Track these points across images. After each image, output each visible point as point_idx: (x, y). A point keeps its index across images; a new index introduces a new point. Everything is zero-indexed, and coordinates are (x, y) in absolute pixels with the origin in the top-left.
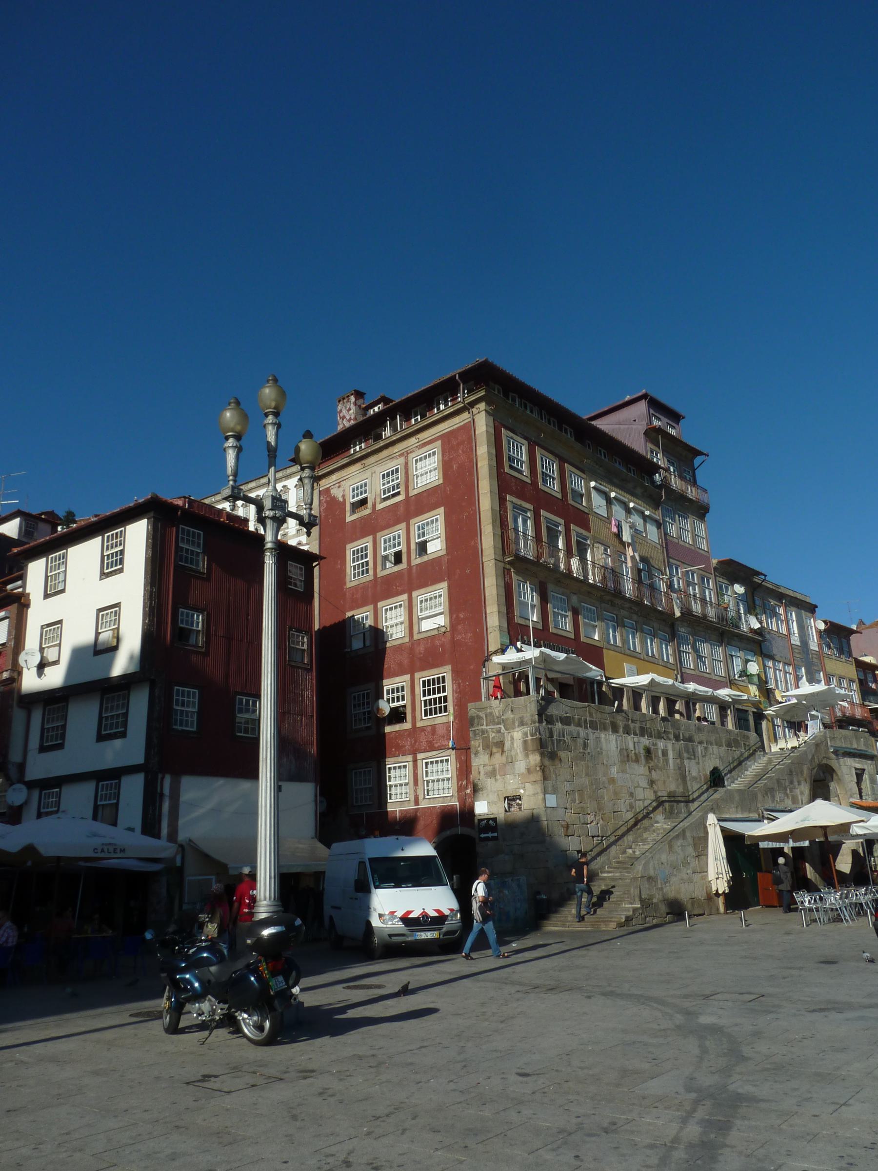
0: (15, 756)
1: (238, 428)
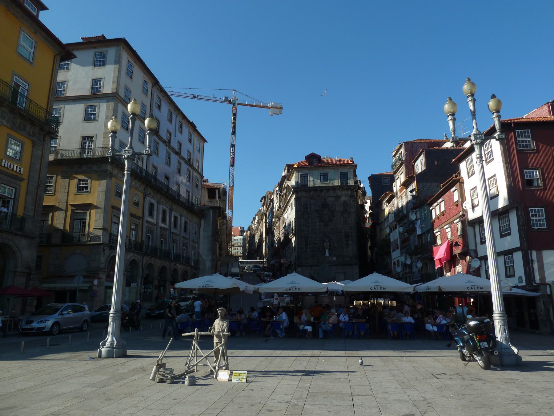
1: (452, 110)
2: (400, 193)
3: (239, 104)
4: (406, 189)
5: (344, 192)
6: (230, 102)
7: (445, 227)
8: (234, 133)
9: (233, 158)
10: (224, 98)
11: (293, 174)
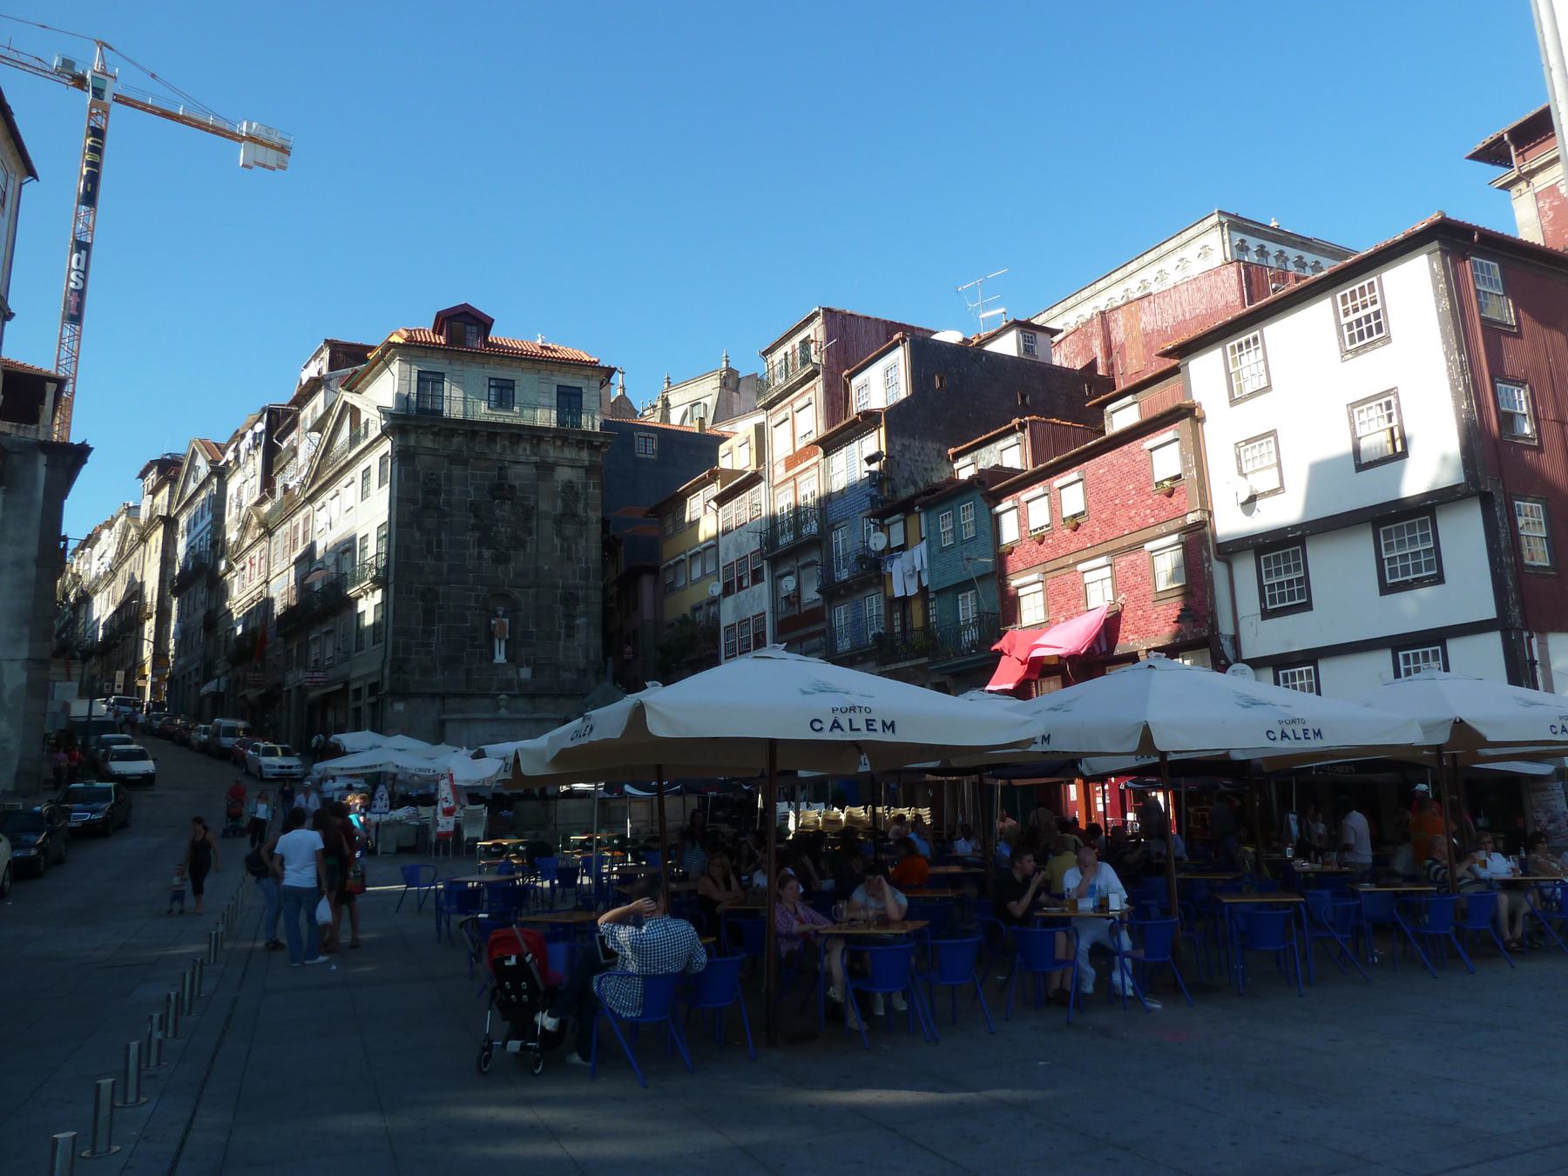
0: (1226, 628)
2: (787, 469)
3: (118, 99)
4: (826, 455)
5: (569, 453)
6: (80, 82)
7: (1081, 567)
8: (89, 198)
9: (81, 293)
10: (56, 62)
11: (387, 365)
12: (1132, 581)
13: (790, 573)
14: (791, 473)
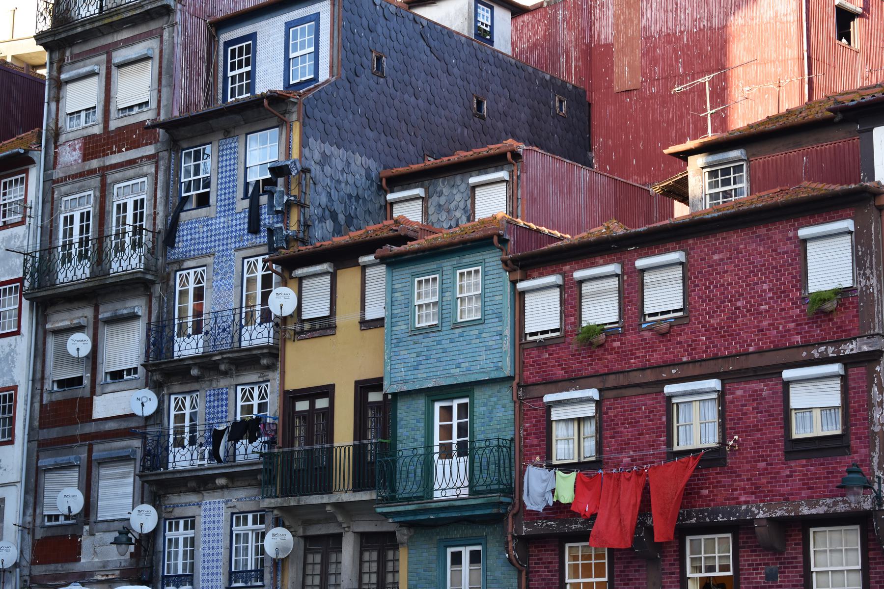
2: (87, 155)
12: (753, 418)
13: (79, 328)
14: (95, 164)
